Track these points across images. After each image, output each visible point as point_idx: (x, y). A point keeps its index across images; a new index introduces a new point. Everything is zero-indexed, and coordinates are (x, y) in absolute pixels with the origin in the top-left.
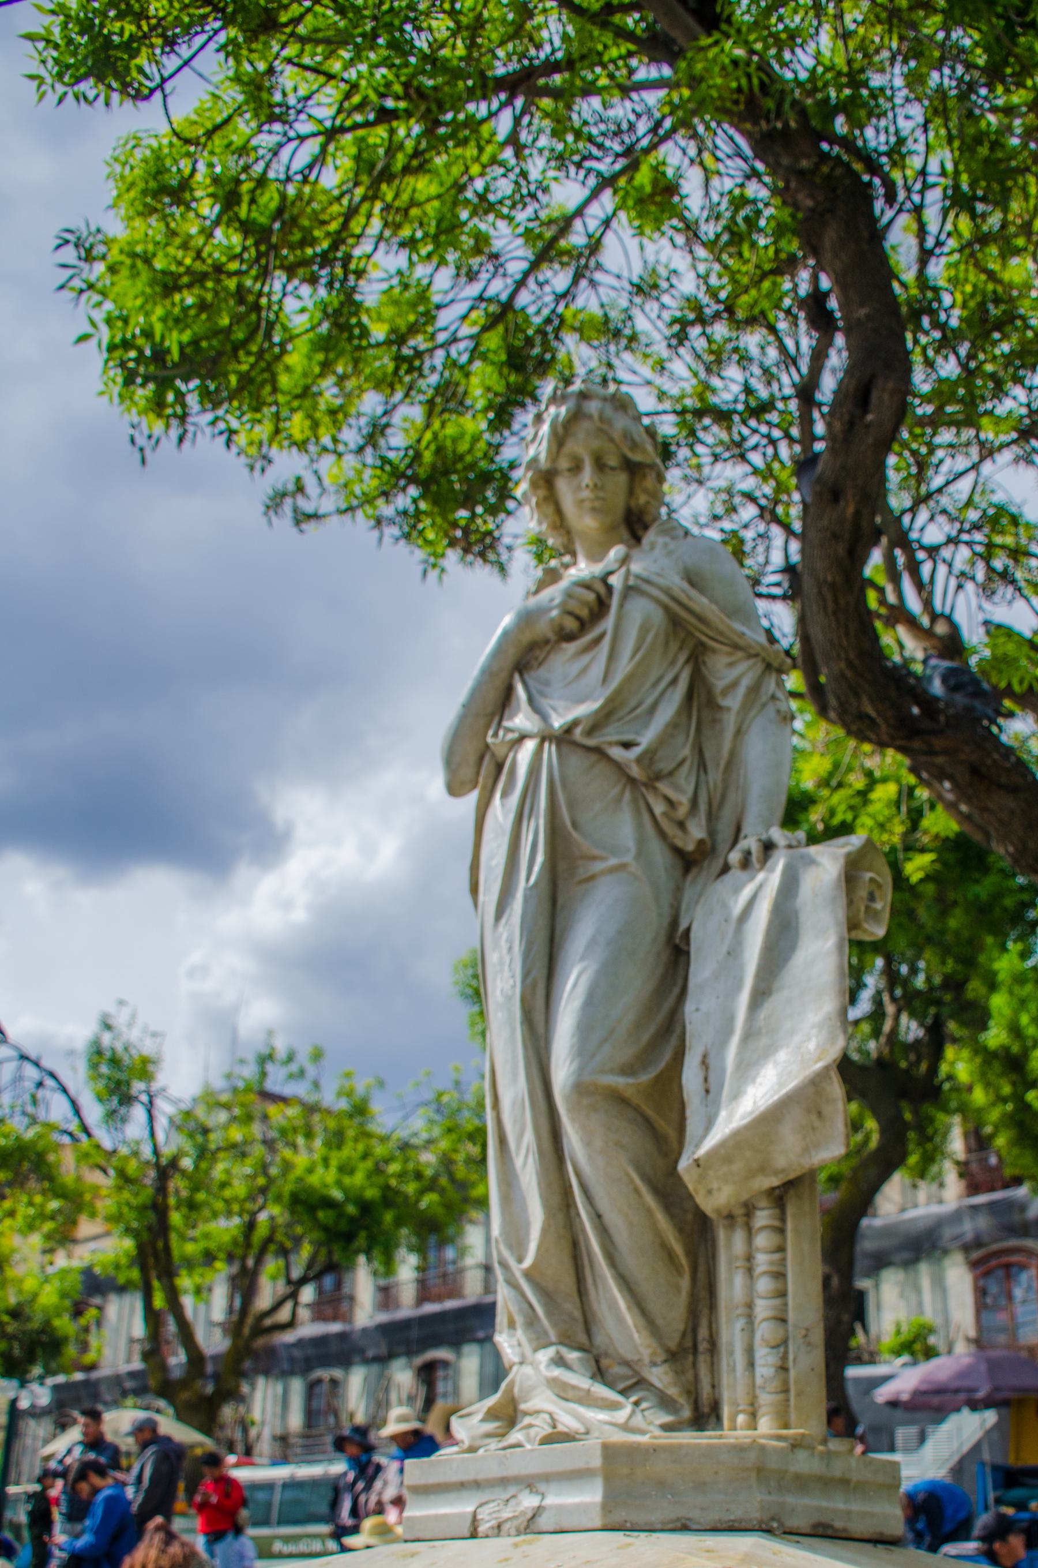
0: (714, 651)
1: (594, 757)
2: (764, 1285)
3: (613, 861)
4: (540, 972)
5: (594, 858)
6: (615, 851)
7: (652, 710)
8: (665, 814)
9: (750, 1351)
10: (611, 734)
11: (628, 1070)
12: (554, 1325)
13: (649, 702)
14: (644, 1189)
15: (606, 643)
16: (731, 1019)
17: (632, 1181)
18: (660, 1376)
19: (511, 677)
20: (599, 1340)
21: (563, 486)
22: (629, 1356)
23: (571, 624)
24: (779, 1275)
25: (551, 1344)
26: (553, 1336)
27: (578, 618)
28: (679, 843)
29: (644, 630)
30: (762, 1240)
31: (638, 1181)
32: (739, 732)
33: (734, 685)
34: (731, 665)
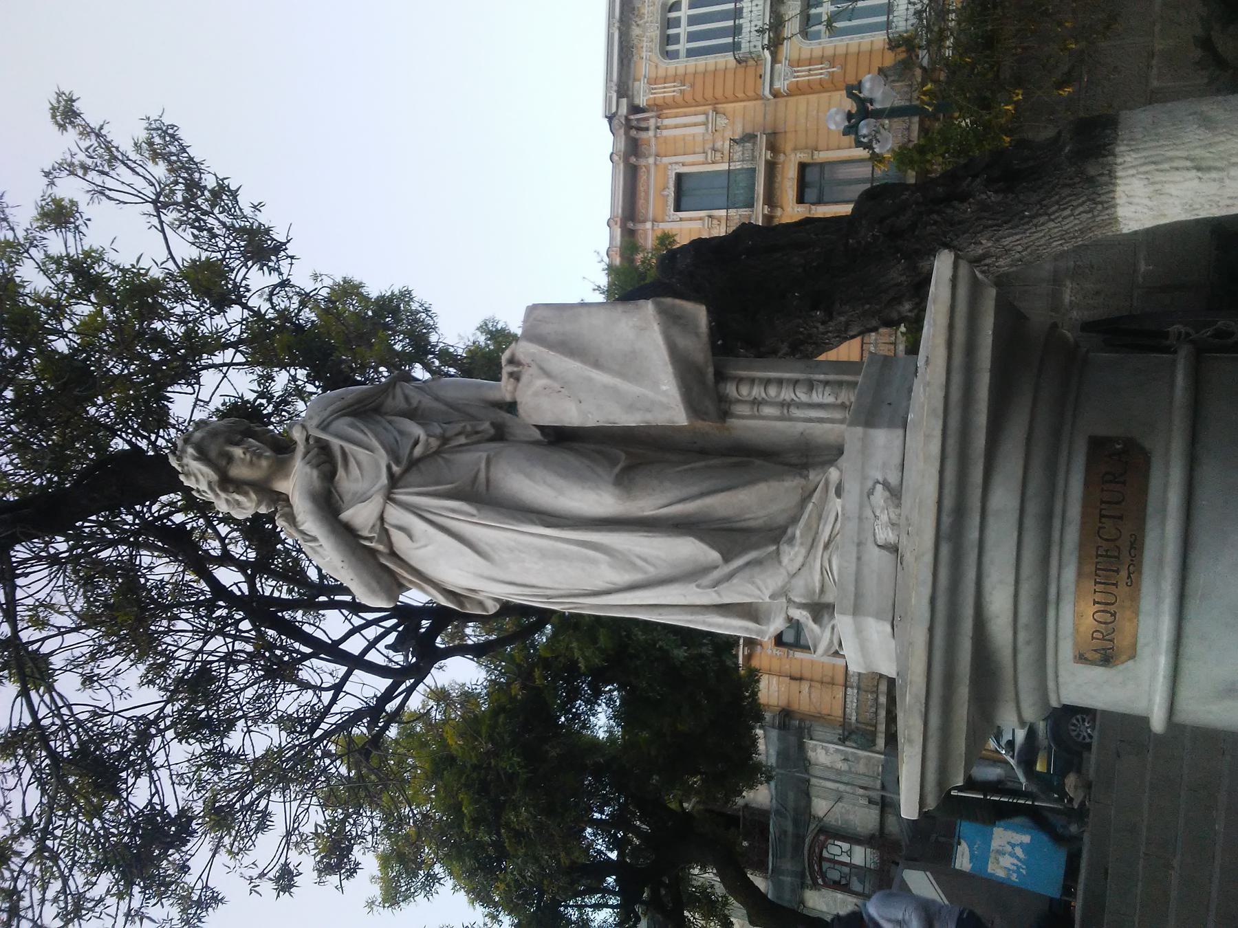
0: (381, 405)
1: (414, 469)
2: (772, 391)
3: (483, 465)
4: (533, 517)
5: (475, 478)
7: (401, 433)
8: (467, 437)
10: (404, 453)
11: (613, 462)
12: (766, 545)
13: (396, 433)
14: (693, 465)
15: (349, 447)
16: (606, 387)
17: (686, 470)
18: (813, 476)
20: (781, 520)
23: (327, 467)
24: (767, 382)
25: (778, 549)
27: (324, 462)
28: (487, 436)
29: (352, 426)
30: (744, 390)
31: (686, 467)
32: (437, 399)
33: (407, 398)
34: (394, 398)
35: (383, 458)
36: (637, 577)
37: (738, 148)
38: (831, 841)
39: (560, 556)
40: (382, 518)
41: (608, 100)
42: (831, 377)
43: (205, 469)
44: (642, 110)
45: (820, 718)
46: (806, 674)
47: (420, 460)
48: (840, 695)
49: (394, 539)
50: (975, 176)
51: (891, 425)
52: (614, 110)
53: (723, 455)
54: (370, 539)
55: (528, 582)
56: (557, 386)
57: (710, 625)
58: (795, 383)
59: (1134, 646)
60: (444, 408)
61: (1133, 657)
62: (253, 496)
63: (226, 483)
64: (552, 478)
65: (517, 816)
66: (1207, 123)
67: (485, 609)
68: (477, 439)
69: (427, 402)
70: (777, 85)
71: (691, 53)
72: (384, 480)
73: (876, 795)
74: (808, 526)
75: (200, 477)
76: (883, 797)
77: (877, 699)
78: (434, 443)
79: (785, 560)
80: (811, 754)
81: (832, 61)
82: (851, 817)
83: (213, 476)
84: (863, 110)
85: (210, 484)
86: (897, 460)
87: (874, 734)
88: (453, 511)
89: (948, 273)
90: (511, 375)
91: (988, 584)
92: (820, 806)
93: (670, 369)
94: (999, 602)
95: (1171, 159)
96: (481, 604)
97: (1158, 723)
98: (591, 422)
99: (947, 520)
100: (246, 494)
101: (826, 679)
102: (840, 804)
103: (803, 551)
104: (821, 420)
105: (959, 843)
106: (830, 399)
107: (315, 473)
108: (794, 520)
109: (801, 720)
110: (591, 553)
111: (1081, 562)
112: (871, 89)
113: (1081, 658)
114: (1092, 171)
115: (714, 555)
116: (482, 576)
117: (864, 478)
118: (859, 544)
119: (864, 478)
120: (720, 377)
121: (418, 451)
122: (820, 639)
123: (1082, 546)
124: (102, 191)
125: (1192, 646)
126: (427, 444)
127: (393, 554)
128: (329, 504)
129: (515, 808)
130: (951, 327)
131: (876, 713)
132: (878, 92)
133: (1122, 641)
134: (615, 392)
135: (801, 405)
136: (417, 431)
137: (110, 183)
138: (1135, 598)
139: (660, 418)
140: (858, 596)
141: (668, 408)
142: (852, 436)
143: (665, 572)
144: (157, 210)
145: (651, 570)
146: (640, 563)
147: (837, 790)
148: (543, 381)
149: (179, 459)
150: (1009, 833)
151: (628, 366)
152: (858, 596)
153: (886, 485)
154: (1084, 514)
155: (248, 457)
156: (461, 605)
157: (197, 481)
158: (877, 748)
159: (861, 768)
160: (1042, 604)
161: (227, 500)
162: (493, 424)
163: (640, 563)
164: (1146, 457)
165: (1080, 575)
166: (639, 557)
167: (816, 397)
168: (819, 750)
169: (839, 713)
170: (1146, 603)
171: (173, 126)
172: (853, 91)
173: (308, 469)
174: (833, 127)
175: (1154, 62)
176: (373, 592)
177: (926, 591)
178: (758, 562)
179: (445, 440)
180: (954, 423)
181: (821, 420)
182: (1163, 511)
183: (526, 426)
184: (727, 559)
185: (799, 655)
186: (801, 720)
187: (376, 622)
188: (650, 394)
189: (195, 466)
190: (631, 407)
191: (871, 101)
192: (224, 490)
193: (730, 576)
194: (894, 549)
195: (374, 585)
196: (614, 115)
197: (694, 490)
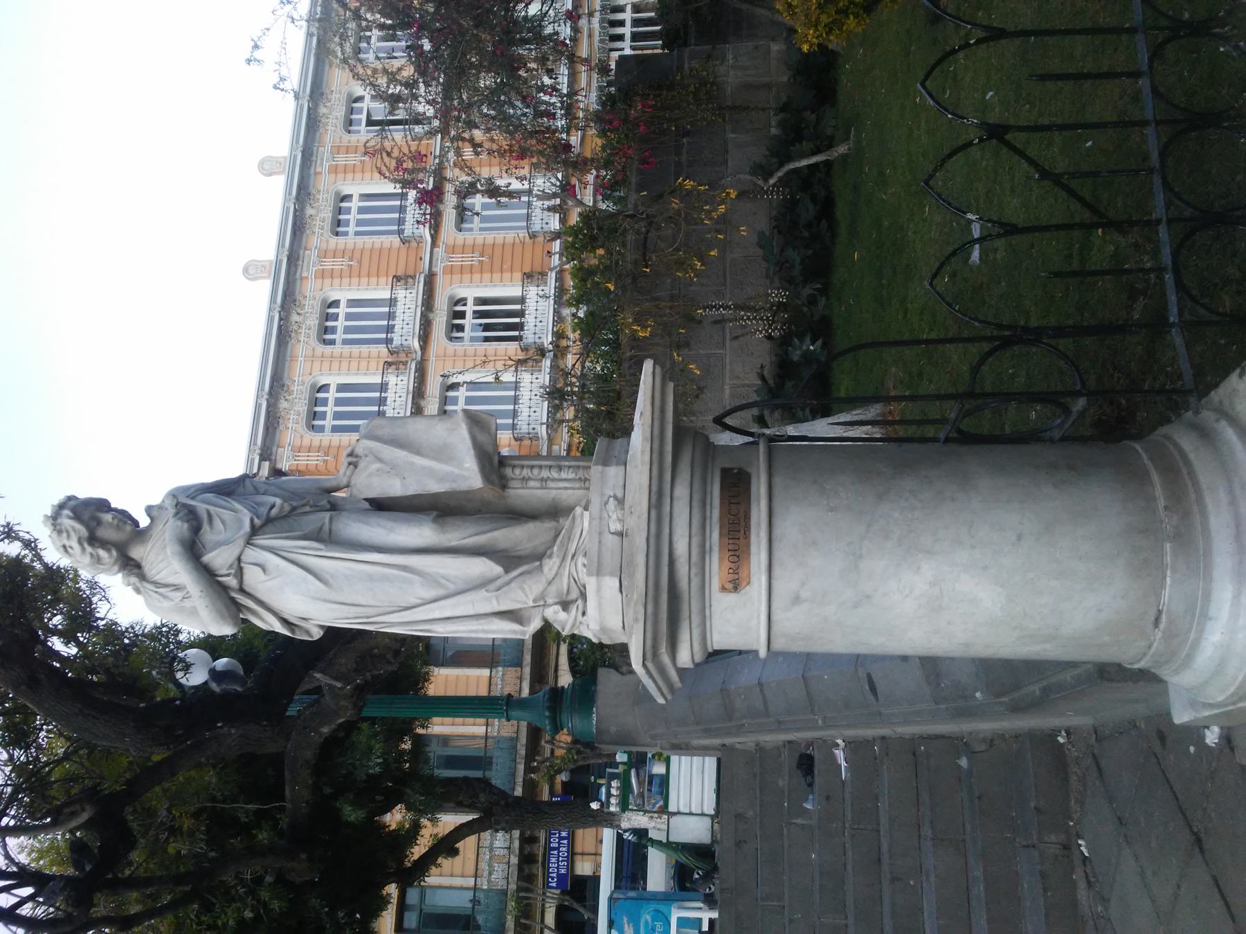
2: (536, 471)
3: (327, 521)
5: (321, 528)
7: (257, 504)
16: (424, 468)
19: (201, 563)
20: (541, 549)
21: (103, 533)
22: (552, 534)
26: (537, 563)
30: (517, 471)
36: (442, 592)
40: (239, 560)
43: (78, 526)
44: (285, 474)
49: (246, 577)
51: (618, 464)
52: (255, 471)
53: (502, 513)
54: (228, 575)
55: (356, 602)
57: (488, 632)
58: (550, 467)
59: (749, 576)
61: (749, 583)
62: (114, 553)
64: (383, 522)
67: (310, 635)
71: (335, 429)
72: (247, 528)
75: (72, 534)
78: (287, 508)
79: (546, 569)
83: (84, 532)
86: (621, 483)
88: (304, 548)
89: (651, 370)
90: (350, 464)
91: (675, 538)
93: (472, 452)
94: (681, 547)
96: (308, 633)
100: (109, 551)
104: (566, 488)
106: (572, 476)
107: (186, 525)
108: (551, 547)
111: (721, 528)
113: (723, 589)
115: (498, 569)
116: (318, 599)
117: (603, 495)
118: (600, 533)
119: (603, 495)
121: (274, 512)
122: (567, 621)
125: (777, 571)
126: (282, 508)
127: (242, 590)
133: (743, 574)
134: (431, 473)
135: (553, 480)
136: (271, 499)
138: (748, 546)
139: (462, 486)
143: (461, 586)
151: (442, 453)
153: (615, 497)
154: (722, 503)
155: (116, 521)
156: (293, 632)
157: (69, 536)
160: (703, 552)
161: (92, 555)
162: (329, 502)
163: (443, 581)
165: (721, 535)
166: (443, 577)
167: (564, 475)
170: (753, 549)
173: (179, 523)
176: (223, 617)
177: (645, 535)
178: (529, 572)
180: (656, 446)
181: (566, 488)
183: (359, 501)
184: (507, 571)
188: (456, 471)
190: (441, 480)
193: (508, 583)
194: (621, 534)
195: (224, 610)
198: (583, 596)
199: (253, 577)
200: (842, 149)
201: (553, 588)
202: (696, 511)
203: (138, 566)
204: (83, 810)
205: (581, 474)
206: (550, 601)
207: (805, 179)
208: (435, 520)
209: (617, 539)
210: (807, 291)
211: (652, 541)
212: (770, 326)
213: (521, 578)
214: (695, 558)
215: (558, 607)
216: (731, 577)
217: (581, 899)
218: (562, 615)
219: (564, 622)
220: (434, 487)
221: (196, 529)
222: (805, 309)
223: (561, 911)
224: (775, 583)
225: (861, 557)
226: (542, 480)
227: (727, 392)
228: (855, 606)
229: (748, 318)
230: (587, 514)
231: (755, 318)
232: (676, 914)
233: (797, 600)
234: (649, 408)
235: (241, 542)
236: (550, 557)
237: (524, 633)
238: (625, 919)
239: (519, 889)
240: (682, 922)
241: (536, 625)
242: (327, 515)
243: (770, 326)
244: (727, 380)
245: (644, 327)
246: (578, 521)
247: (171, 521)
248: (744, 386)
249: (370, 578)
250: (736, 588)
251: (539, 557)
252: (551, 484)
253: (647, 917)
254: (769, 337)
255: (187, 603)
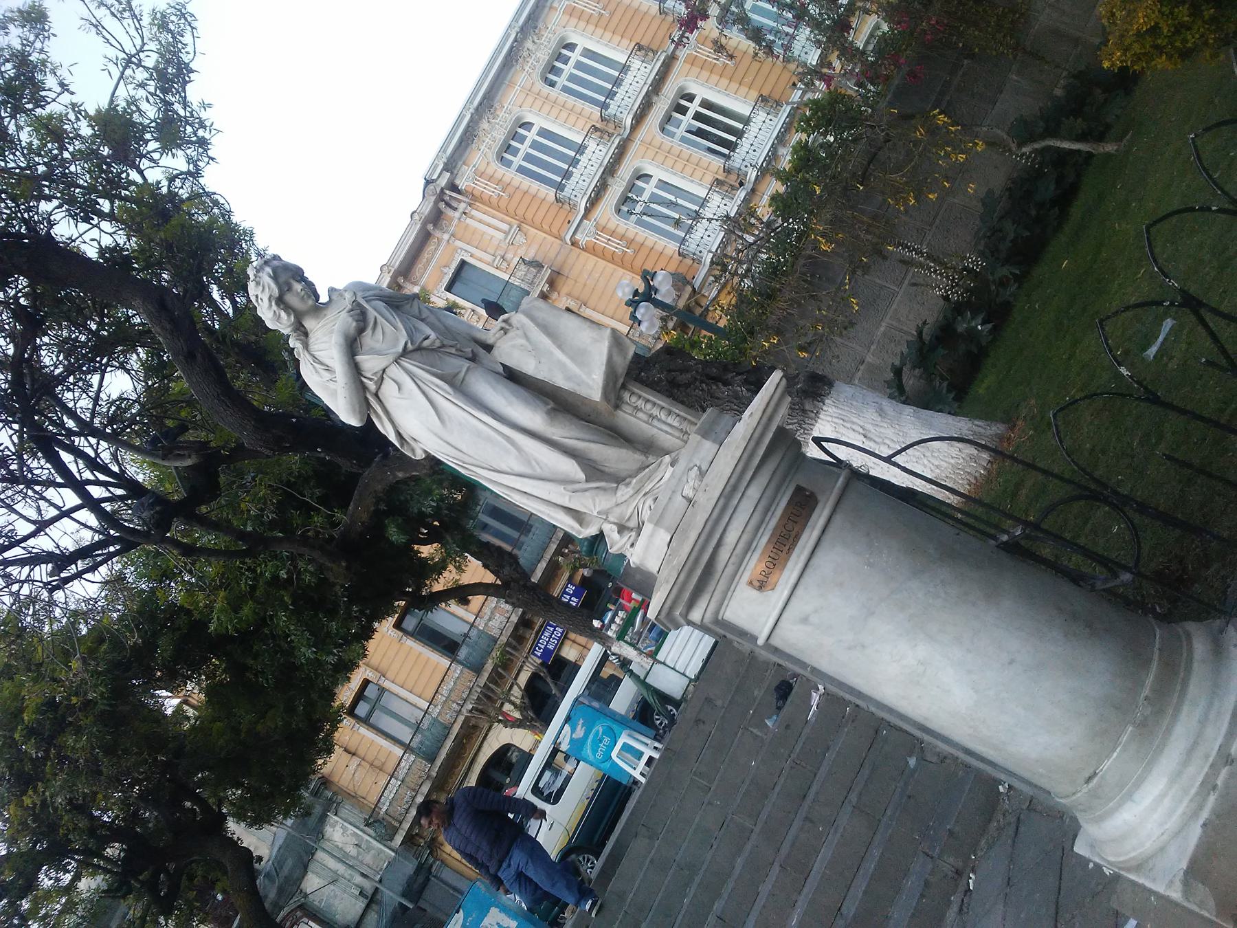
2: (649, 406)
3: (464, 370)
6: (461, 367)
9: (665, 423)
11: (547, 404)
16: (559, 361)
18: (651, 459)
20: (624, 474)
22: (637, 466)
23: (362, 324)
30: (634, 399)
35: (403, 338)
37: (523, 267)
38: (305, 920)
39: (488, 439)
40: (384, 371)
41: (433, 166)
42: (682, 414)
43: (273, 285)
44: (459, 192)
45: (353, 797)
46: (361, 752)
47: (425, 349)
48: (383, 783)
50: (739, 374)
51: (714, 441)
53: (605, 427)
54: (371, 380)
56: (530, 348)
57: (552, 518)
60: (441, 326)
62: (292, 318)
63: (280, 301)
64: (507, 394)
65: (76, 741)
66: (881, 412)
68: (461, 354)
69: (432, 319)
70: (578, 236)
71: (521, 170)
72: (400, 349)
73: (368, 886)
74: (641, 481)
76: (377, 889)
77: (414, 798)
78: (438, 344)
79: (619, 493)
80: (328, 830)
81: (630, 243)
82: (337, 902)
83: (276, 293)
84: (647, 295)
85: (270, 296)
87: (395, 831)
91: (730, 528)
92: (312, 882)
93: (604, 368)
94: (732, 537)
95: (853, 423)
96: (413, 451)
97: (761, 642)
98: (541, 375)
99: (728, 488)
100: (289, 315)
101: (377, 763)
102: (332, 887)
103: (632, 492)
104: (667, 432)
105: (458, 912)
106: (676, 424)
107: (354, 324)
108: (632, 476)
109: (335, 793)
110: (509, 446)
112: (660, 283)
113: (750, 583)
114: (807, 407)
116: (432, 432)
117: (690, 461)
119: (690, 461)
120: (624, 387)
121: (426, 343)
123: (775, 529)
124: (97, 26)
125: (800, 591)
127: (376, 395)
128: (352, 346)
129: (78, 731)
130: (768, 404)
131: (407, 810)
132: (665, 289)
133: (772, 579)
134: (562, 366)
135: (659, 420)
136: (428, 331)
137: (110, 23)
138: (787, 560)
139: (583, 392)
140: (662, 516)
141: (591, 388)
142: (695, 438)
143: (546, 474)
144: (128, 62)
145: (539, 470)
146: (534, 463)
147: (335, 872)
148: (523, 341)
149: (258, 271)
150: (503, 915)
151: (579, 356)
152: (662, 516)
153: (699, 468)
154: (782, 516)
158: (393, 844)
159: (368, 859)
160: (748, 548)
163: (534, 463)
164: (816, 502)
165: (769, 541)
167: (670, 420)
168: (338, 828)
169: (374, 799)
170: (790, 564)
171: (192, 15)
172: (647, 276)
173: (350, 319)
174: (620, 294)
175: (862, 368)
176: (354, 411)
178: (604, 489)
179: (443, 346)
181: (667, 432)
182: (814, 528)
183: (496, 362)
185: (363, 731)
186: (335, 793)
187: (105, 484)
188: (584, 377)
189: (266, 279)
190: (568, 378)
191: (656, 291)
192: (278, 305)
193: (585, 490)
195: (357, 407)
196: (433, 181)
197: (587, 437)
198: (639, 529)
199: (388, 390)
200: (1110, 148)
201: (618, 511)
202: (773, 485)
203: (306, 334)
204: (190, 457)
205: (685, 426)
206: (611, 519)
207: (1062, 158)
208: (548, 413)
209: (685, 503)
210: (1004, 271)
211: (710, 523)
212: (953, 287)
213: (594, 492)
214: (738, 550)
215: (615, 528)
216: (761, 578)
217: (556, 676)
218: (615, 536)
219: (616, 542)
220: (560, 381)
221: (361, 331)
222: (993, 287)
223: (535, 677)
224: (793, 598)
225: (873, 613)
226: (651, 416)
227: (882, 329)
228: (850, 648)
229: (935, 271)
230: (670, 469)
231: (941, 274)
232: (624, 739)
233: (805, 620)
234: (760, 413)
235: (391, 358)
236: (628, 485)
237: (580, 533)
238: (581, 721)
239: (508, 644)
240: (626, 747)
241: (592, 531)
242: (466, 364)
243: (953, 287)
244: (887, 319)
245: (830, 240)
246: (663, 467)
247: (344, 314)
248: (900, 330)
249: (479, 434)
250: (760, 588)
251: (619, 480)
252: (655, 423)
253: (599, 729)
254: (946, 298)
255: (331, 385)
